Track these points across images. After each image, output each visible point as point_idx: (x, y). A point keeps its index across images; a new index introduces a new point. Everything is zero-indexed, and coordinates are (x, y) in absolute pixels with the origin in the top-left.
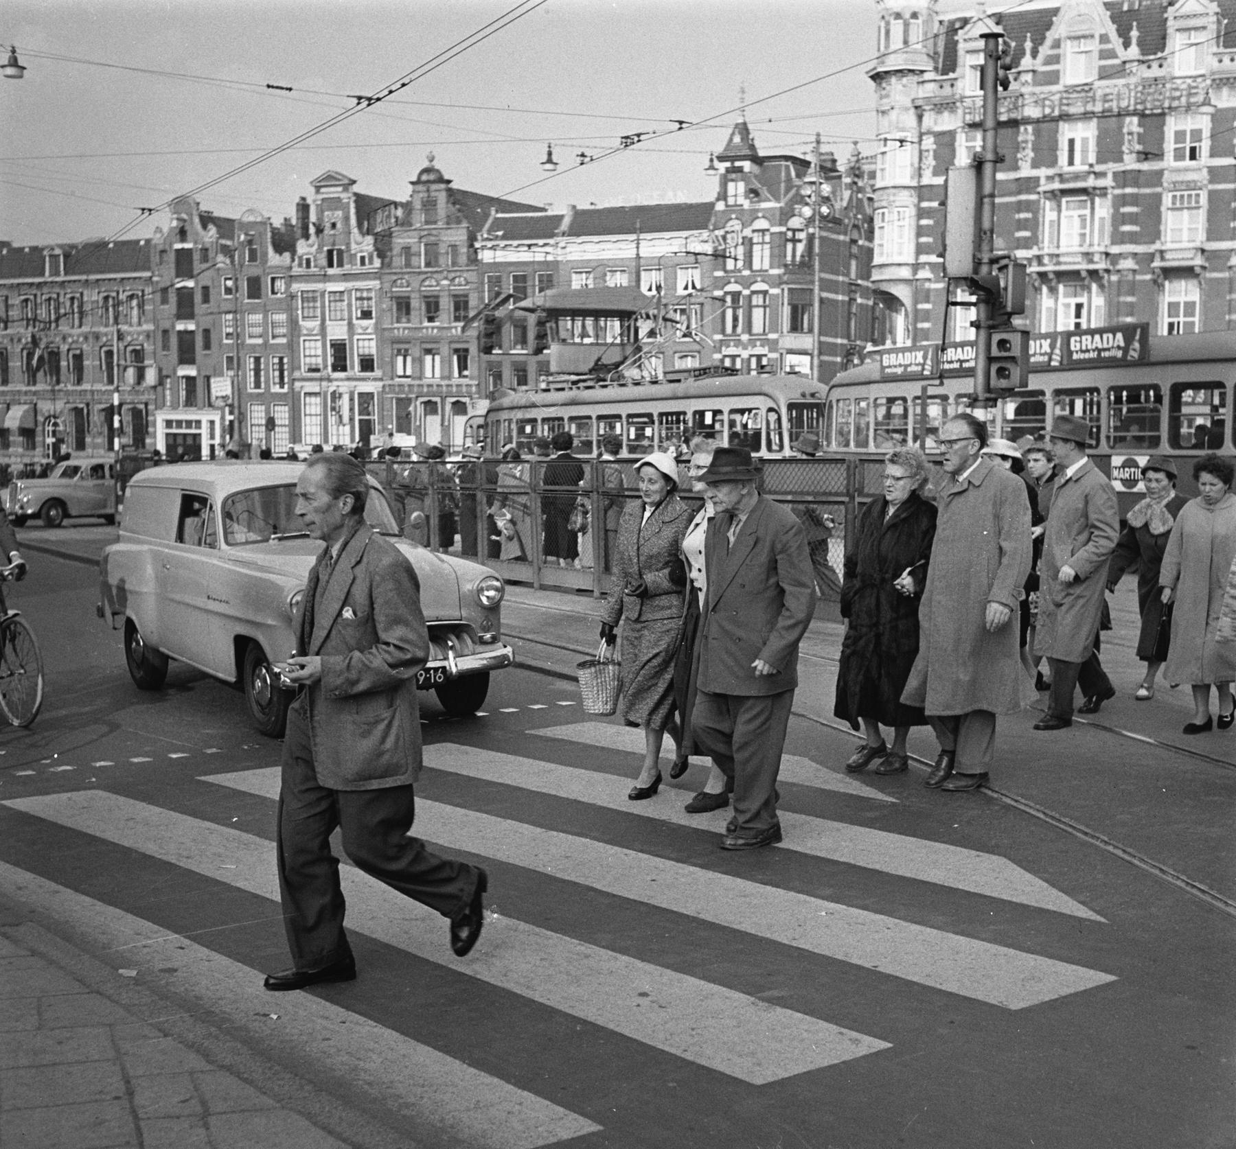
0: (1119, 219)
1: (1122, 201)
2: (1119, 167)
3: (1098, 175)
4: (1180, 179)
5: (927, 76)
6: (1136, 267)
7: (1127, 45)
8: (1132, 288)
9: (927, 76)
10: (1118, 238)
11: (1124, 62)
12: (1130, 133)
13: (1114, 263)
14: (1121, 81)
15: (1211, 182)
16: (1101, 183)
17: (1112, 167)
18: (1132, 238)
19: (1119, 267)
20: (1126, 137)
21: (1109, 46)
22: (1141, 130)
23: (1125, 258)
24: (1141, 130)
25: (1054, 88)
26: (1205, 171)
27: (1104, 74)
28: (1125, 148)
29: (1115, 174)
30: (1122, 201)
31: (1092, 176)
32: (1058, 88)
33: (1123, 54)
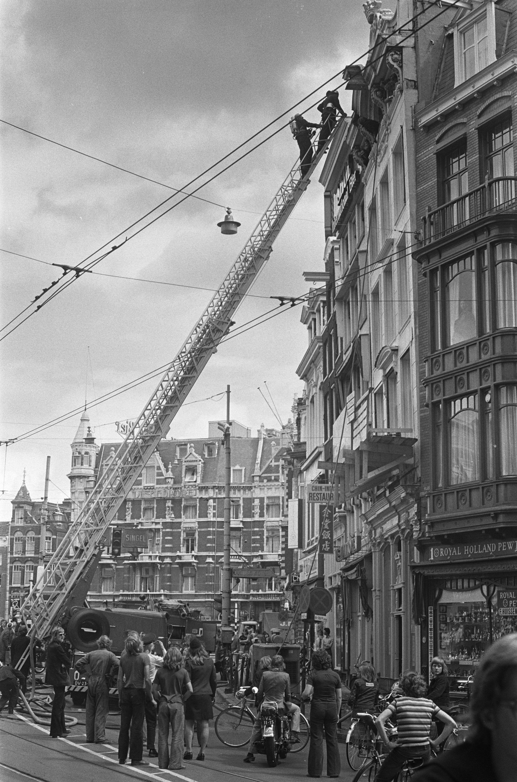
0: (165, 542)
1: (165, 534)
2: (164, 520)
3: (157, 523)
4: (187, 526)
5: (90, 479)
6: (171, 562)
7: (167, 471)
8: (170, 571)
9: (90, 479)
10: (164, 550)
11: (166, 478)
12: (168, 507)
13: (163, 560)
14: (165, 486)
15: (199, 528)
16: (158, 527)
17: (161, 520)
18: (171, 550)
19: (164, 562)
20: (168, 508)
21: (160, 471)
22: (172, 505)
23: (167, 558)
24: (172, 505)
25: (140, 487)
26: (197, 524)
27: (159, 482)
28: (167, 512)
29: (163, 523)
30: (165, 534)
31: (154, 524)
32: (142, 487)
33: (166, 475)
